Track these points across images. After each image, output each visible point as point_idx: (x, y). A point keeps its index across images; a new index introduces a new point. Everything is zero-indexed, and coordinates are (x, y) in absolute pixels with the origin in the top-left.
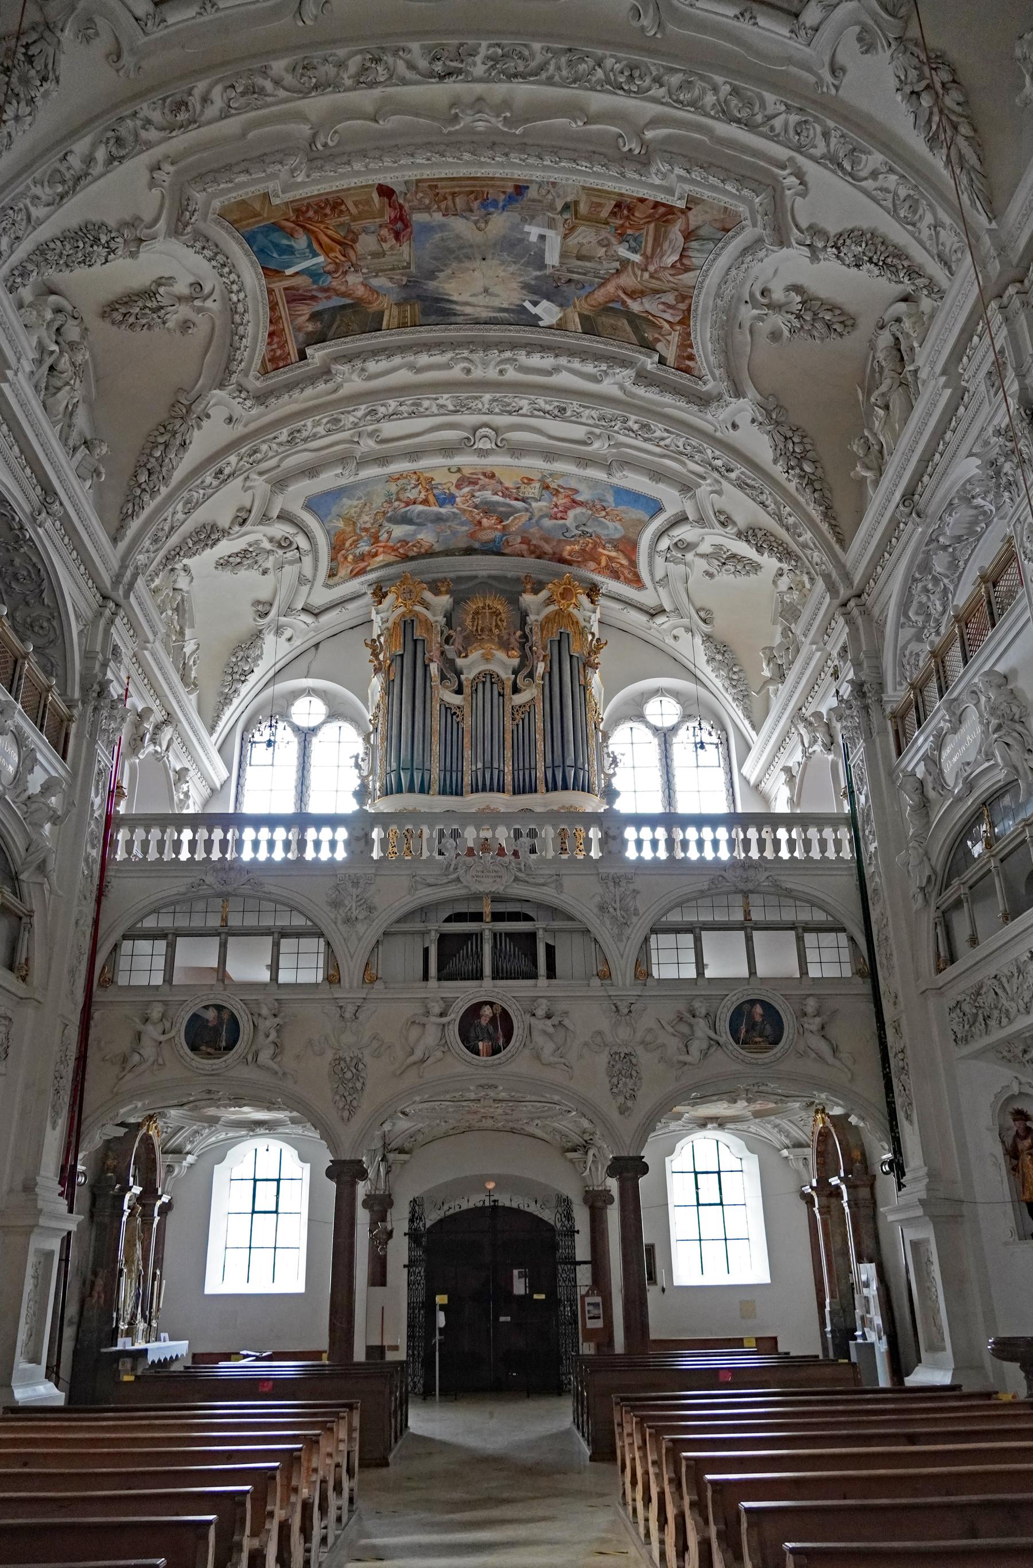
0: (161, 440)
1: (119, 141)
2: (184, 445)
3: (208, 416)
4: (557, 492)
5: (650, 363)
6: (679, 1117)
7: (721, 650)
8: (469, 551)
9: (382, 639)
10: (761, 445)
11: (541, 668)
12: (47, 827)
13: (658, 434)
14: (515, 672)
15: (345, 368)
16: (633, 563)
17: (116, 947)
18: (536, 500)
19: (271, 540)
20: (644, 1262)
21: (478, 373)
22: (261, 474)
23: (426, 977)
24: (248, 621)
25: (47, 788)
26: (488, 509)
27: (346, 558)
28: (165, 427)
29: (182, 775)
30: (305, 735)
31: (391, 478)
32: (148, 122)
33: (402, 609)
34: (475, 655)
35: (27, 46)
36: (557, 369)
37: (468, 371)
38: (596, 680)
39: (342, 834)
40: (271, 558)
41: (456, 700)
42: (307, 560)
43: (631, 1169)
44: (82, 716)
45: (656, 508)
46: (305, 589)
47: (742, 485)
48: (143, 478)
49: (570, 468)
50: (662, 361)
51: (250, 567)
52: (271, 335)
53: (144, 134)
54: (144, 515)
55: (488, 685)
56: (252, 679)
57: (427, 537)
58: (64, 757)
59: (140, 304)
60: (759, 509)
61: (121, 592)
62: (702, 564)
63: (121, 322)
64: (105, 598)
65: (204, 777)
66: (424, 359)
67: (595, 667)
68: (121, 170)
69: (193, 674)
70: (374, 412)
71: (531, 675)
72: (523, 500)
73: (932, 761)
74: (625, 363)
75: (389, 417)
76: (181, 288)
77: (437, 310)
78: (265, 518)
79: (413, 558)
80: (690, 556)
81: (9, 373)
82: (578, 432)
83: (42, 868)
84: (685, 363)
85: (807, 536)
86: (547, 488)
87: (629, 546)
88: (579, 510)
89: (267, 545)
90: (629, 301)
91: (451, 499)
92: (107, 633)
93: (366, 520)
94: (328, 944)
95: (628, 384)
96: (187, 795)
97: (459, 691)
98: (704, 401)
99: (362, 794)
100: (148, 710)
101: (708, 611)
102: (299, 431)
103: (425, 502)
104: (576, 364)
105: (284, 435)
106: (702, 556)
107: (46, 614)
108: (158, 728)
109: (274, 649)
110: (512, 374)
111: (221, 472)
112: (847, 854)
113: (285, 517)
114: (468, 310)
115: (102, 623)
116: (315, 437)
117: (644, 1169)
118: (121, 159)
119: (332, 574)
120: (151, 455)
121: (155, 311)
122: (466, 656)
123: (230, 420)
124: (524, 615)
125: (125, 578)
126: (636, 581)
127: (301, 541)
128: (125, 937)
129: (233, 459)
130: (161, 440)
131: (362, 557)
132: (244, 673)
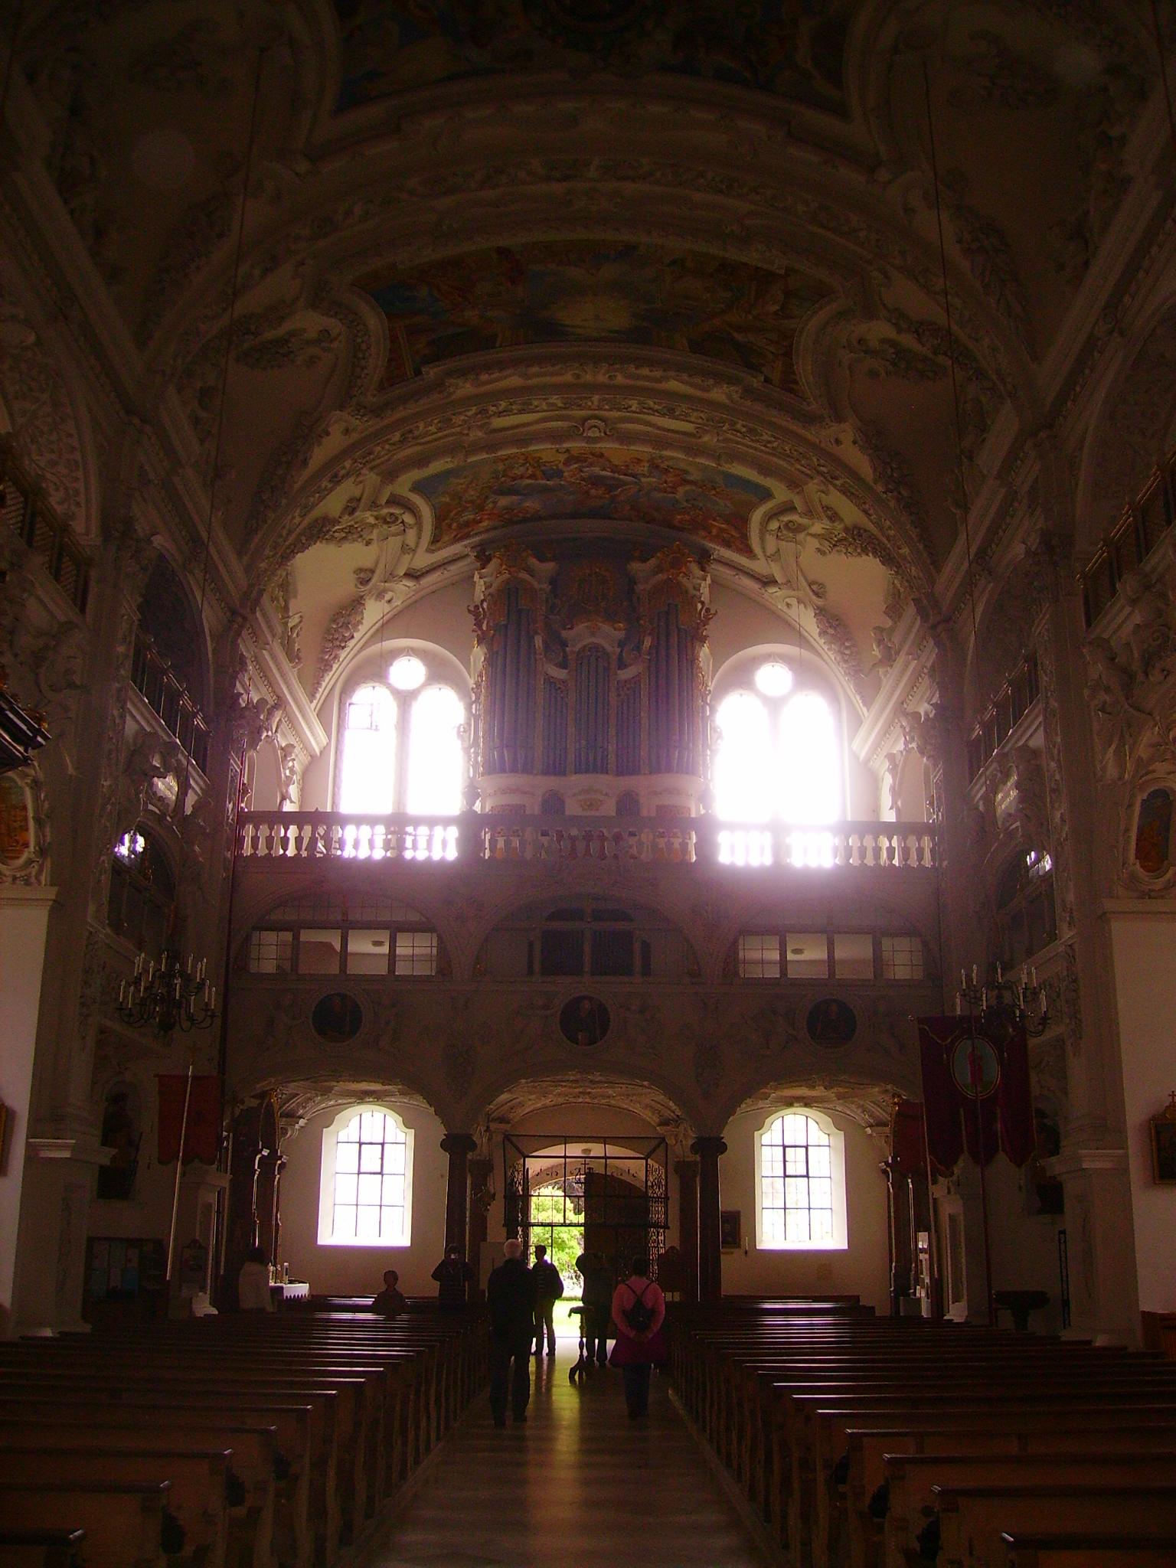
0: (284, 459)
2: (305, 463)
3: (328, 434)
4: (666, 471)
5: (756, 382)
6: (766, 1097)
7: (835, 623)
8: (575, 516)
9: (485, 605)
10: (862, 463)
11: (647, 642)
13: (765, 437)
14: (621, 644)
15: (460, 382)
16: (745, 537)
17: (248, 939)
18: (644, 476)
19: (377, 518)
20: (735, 1226)
21: (588, 377)
22: (372, 469)
23: (530, 972)
24: (348, 586)
26: (596, 481)
27: (450, 526)
29: (287, 751)
30: (405, 699)
31: (497, 460)
33: (507, 576)
34: (581, 627)
36: (668, 379)
37: (578, 376)
38: (704, 652)
39: (453, 833)
40: (375, 531)
41: (560, 674)
42: (411, 536)
43: (711, 1147)
45: (767, 495)
46: (407, 558)
47: (844, 491)
49: (680, 455)
50: (767, 380)
51: (354, 540)
52: (390, 361)
55: (593, 659)
56: (351, 643)
57: (531, 504)
60: (861, 514)
62: (814, 543)
64: (234, 613)
65: (306, 747)
66: (535, 369)
67: (703, 640)
69: (297, 646)
70: (483, 412)
71: (638, 648)
72: (632, 475)
73: (989, 800)
74: (731, 381)
75: (500, 414)
76: (312, 334)
77: (552, 332)
78: (374, 505)
79: (520, 522)
80: (801, 536)
82: (689, 427)
84: (789, 382)
85: (905, 551)
86: (657, 467)
87: (740, 521)
88: (688, 488)
89: (372, 520)
90: (735, 334)
91: (559, 474)
92: (235, 645)
93: (472, 493)
94: (440, 938)
95: (735, 396)
96: (292, 770)
97: (563, 665)
98: (809, 419)
99: (472, 794)
100: (263, 701)
101: (821, 585)
102: (411, 431)
103: (533, 476)
104: (685, 376)
105: (397, 437)
106: (814, 536)
108: (270, 714)
109: (373, 612)
110: (620, 379)
111: (336, 475)
112: (927, 862)
113: (390, 502)
114: (579, 331)
116: (427, 434)
117: (723, 1148)
119: (435, 540)
121: (284, 355)
122: (571, 628)
123: (347, 431)
124: (632, 581)
126: (748, 552)
127: (408, 518)
128: (255, 928)
129: (348, 464)
130: (284, 459)
131: (467, 524)
132: (346, 640)
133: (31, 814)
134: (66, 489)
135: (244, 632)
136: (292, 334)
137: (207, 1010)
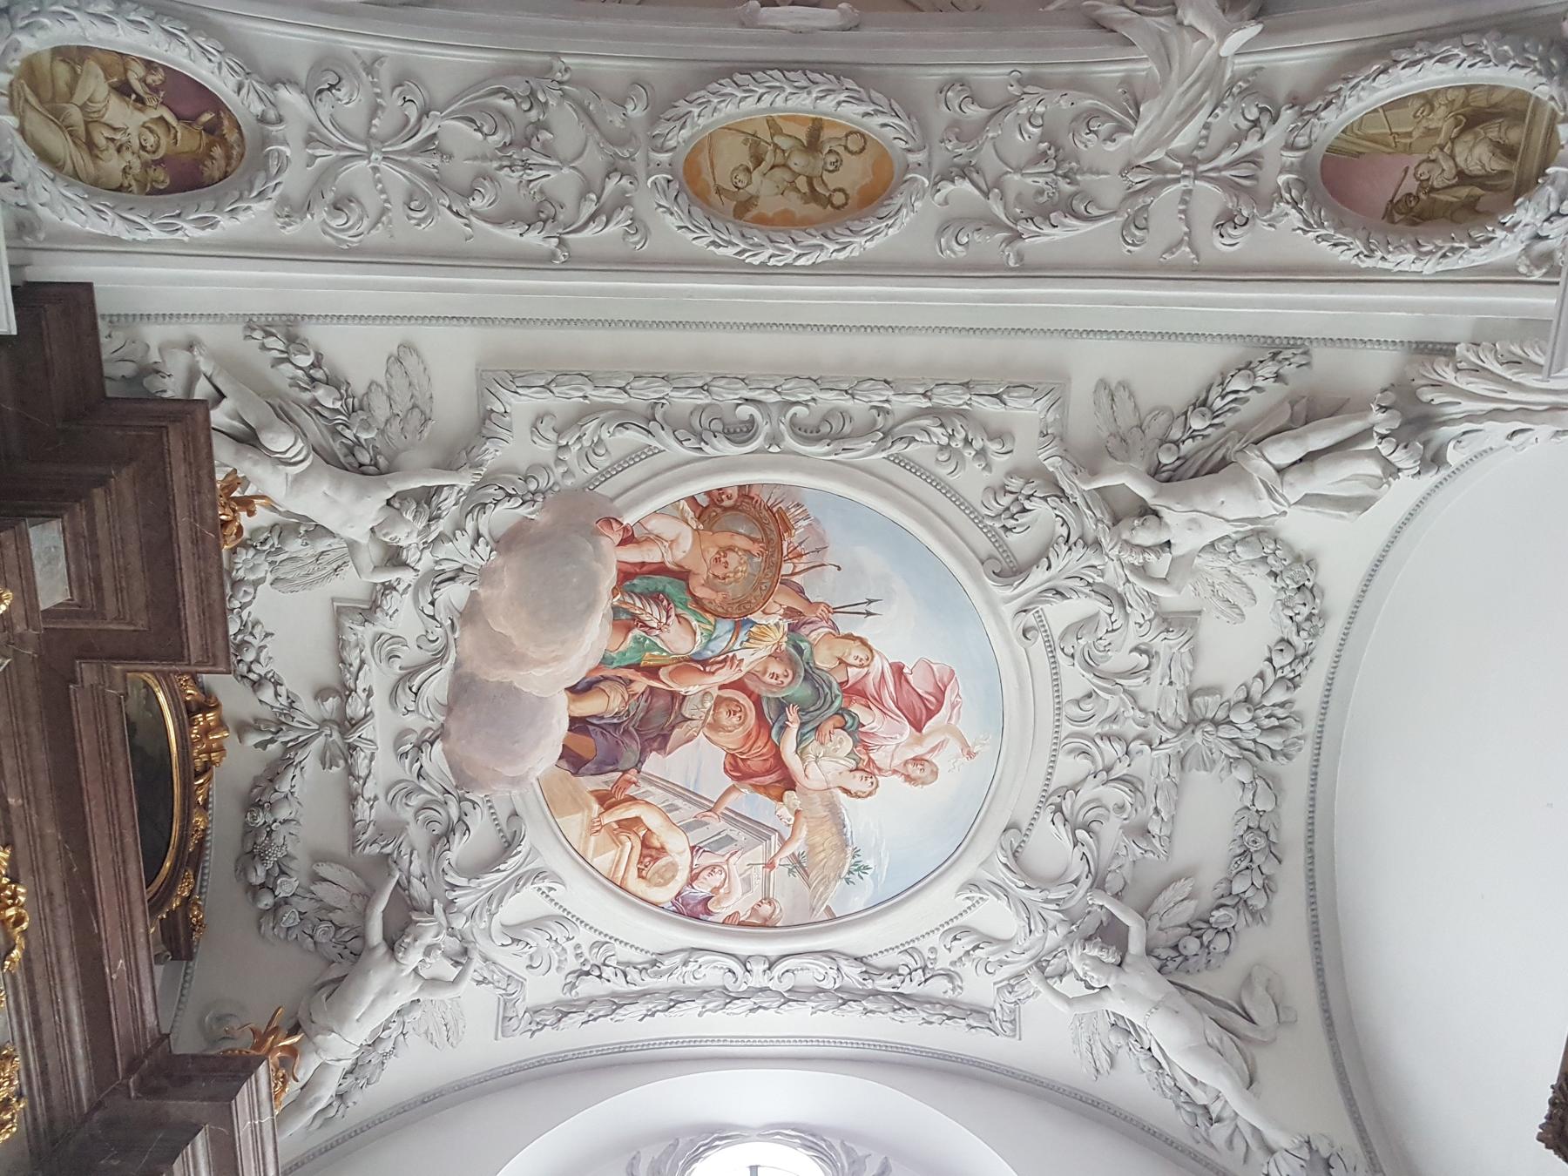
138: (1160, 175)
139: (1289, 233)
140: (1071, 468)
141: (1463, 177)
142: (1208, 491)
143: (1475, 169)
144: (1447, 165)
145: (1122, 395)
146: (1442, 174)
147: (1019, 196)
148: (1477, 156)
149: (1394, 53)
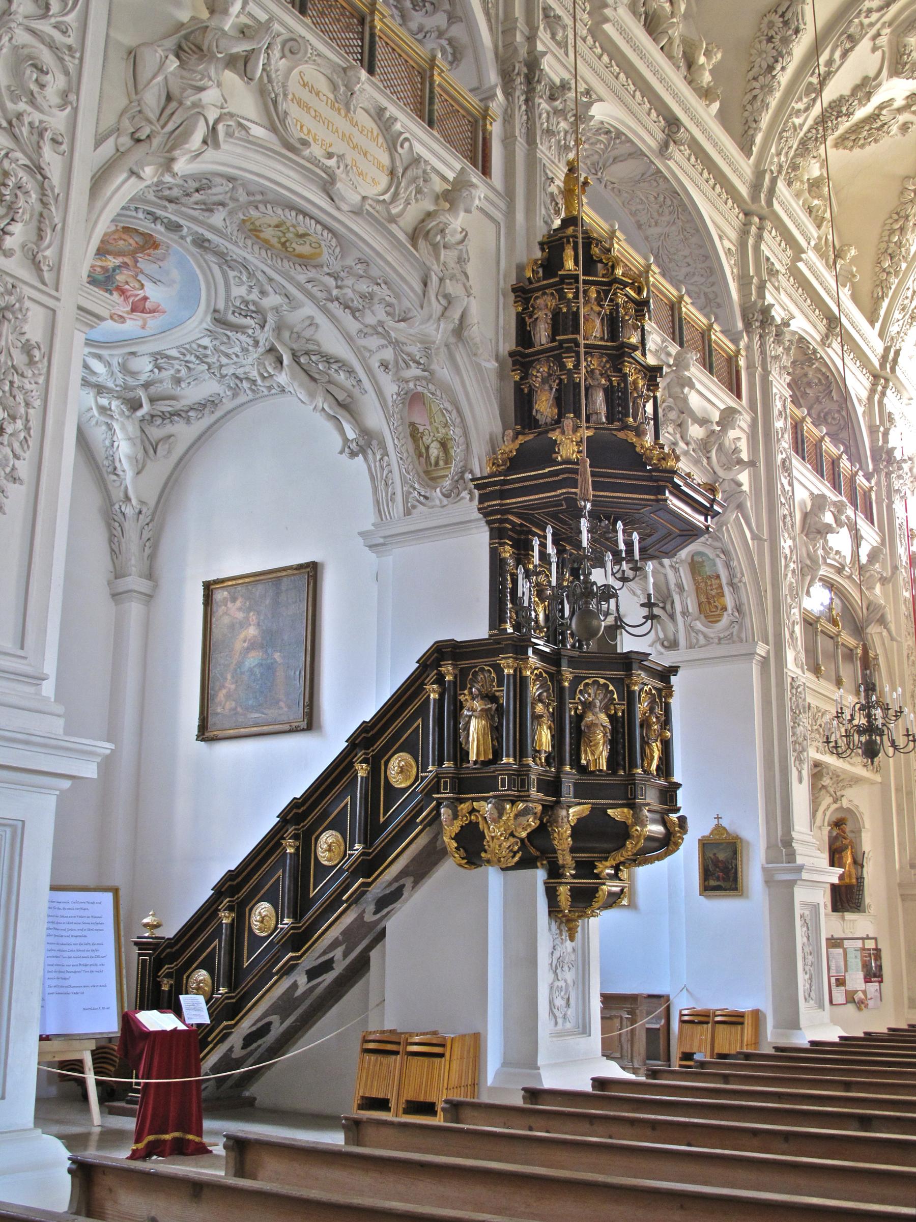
0: (897, 226)
1: (850, 38)
12: (878, 586)
25: (874, 556)
28: (897, 213)
32: (870, 11)
35: (782, 16)
44: (878, 483)
48: (886, 264)
53: (866, 21)
54: (891, 293)
58: (872, 523)
59: (867, 128)
61: (888, 370)
63: (852, 147)
64: (876, 377)
68: (852, 56)
76: (899, 102)
81: (803, 256)
83: (882, 621)
92: (881, 403)
107: (835, 407)
115: (877, 397)
118: (851, 49)
120: (889, 241)
125: (890, 358)
133: (724, 580)
134: (705, 294)
135: (888, 392)
136: (881, 107)
137: (908, 735)
138: (386, 335)
139: (391, 389)
140: (274, 326)
141: (427, 448)
142: (301, 385)
143: (430, 453)
144: (430, 441)
145: (313, 328)
146: (427, 440)
147: (346, 294)
148: (434, 451)
149: (455, 411)
